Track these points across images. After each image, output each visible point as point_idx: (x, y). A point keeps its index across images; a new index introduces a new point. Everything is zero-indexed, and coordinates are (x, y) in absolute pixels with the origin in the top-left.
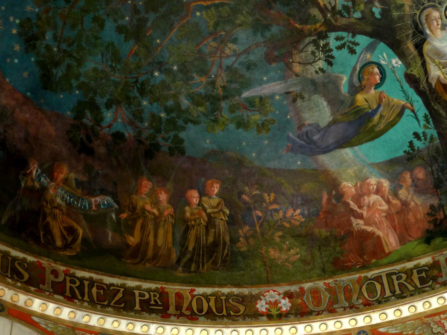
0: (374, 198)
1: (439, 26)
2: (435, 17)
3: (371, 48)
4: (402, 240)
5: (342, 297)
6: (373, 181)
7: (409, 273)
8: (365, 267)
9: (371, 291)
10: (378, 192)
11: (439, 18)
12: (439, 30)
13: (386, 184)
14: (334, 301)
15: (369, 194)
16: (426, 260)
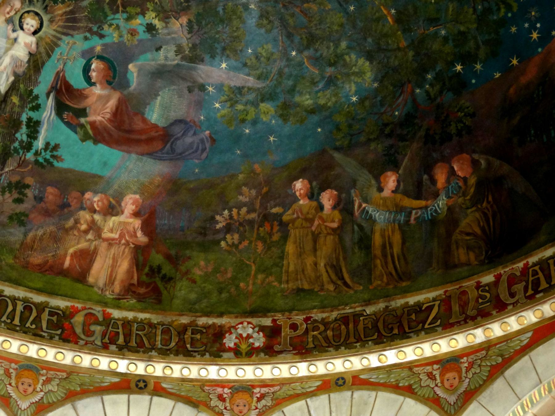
1: (8, 16)
2: (14, 5)
11: (15, 10)
12: (4, 18)
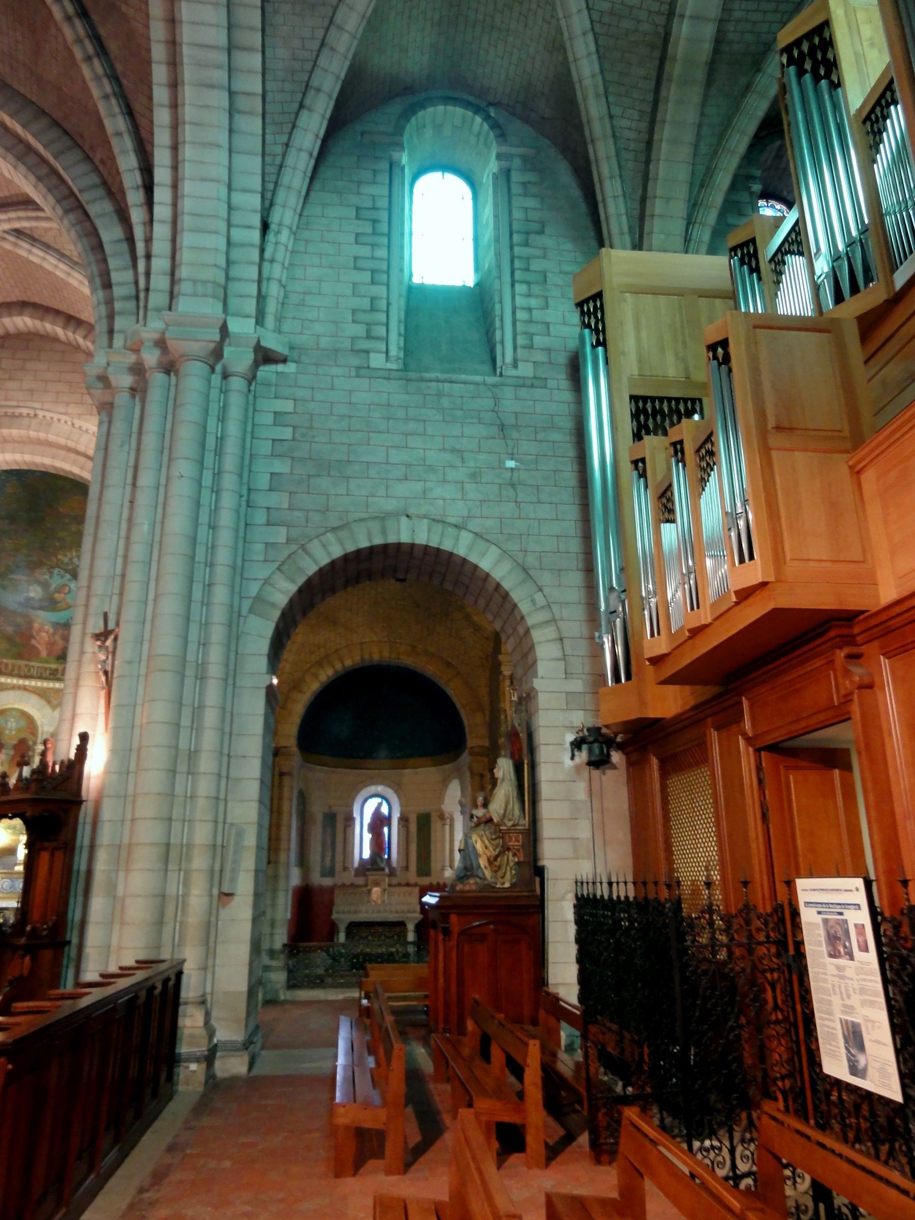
0: (44, 634)
3: (70, 580)
4: (49, 654)
5: (16, 668)
6: (46, 627)
7: (46, 669)
8: (29, 660)
9: (29, 670)
10: (47, 632)
13: (51, 630)
14: (13, 670)
15: (44, 631)
16: (53, 666)
